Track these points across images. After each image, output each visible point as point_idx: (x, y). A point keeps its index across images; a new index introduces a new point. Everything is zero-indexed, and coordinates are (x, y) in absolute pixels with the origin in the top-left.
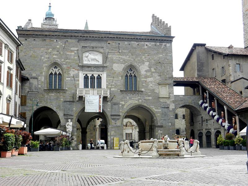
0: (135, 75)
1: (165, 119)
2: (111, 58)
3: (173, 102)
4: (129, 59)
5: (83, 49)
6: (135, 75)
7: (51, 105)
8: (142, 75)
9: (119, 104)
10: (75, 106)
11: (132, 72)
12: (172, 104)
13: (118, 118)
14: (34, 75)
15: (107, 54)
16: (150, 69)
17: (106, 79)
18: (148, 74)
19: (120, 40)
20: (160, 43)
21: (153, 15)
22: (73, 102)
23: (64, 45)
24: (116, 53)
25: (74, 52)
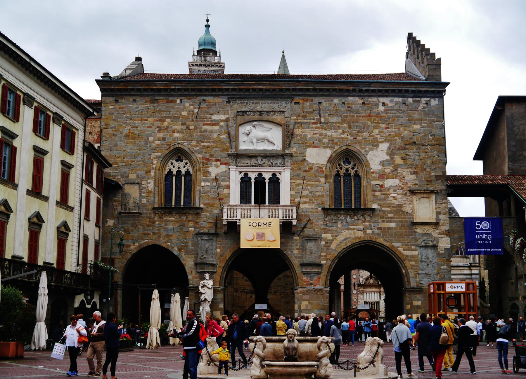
0: (356, 171)
1: (426, 274)
2: (301, 135)
3: (448, 233)
5: (239, 118)
7: (168, 241)
9: (321, 239)
10: (221, 244)
11: (351, 166)
12: (444, 239)
13: (316, 270)
14: (132, 176)
15: (291, 127)
16: (392, 158)
17: (291, 183)
19: (322, 96)
20: (414, 99)
21: (410, 35)
22: (216, 234)
23: (196, 111)
24: (313, 123)
25: (218, 124)
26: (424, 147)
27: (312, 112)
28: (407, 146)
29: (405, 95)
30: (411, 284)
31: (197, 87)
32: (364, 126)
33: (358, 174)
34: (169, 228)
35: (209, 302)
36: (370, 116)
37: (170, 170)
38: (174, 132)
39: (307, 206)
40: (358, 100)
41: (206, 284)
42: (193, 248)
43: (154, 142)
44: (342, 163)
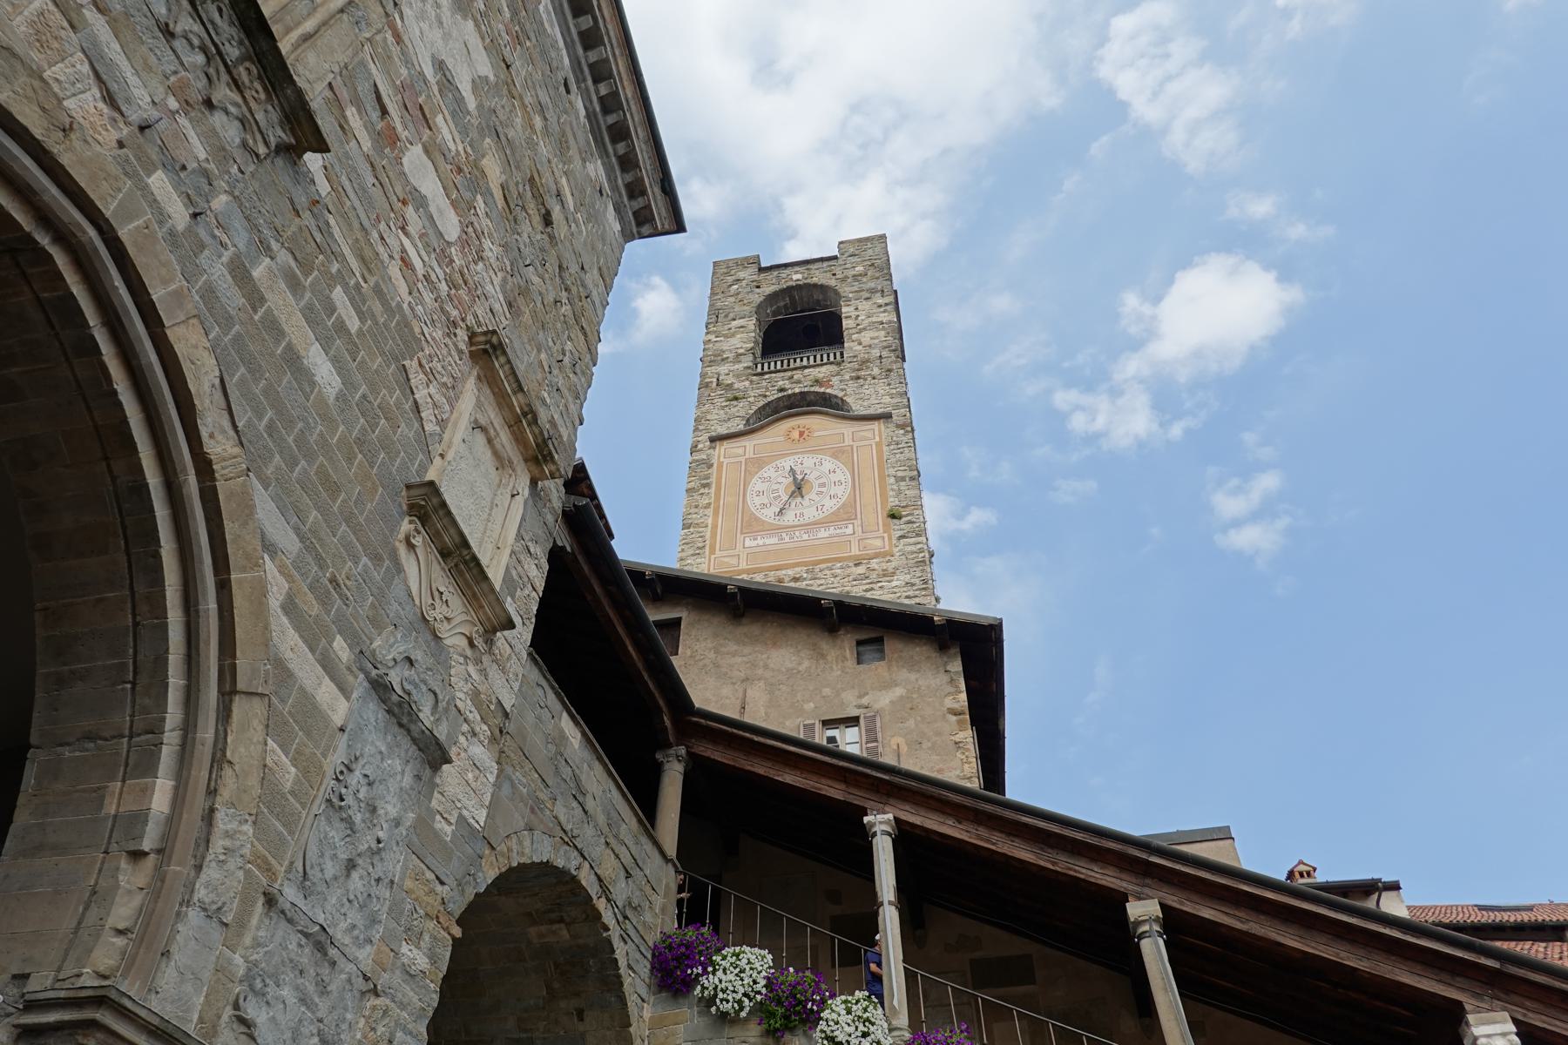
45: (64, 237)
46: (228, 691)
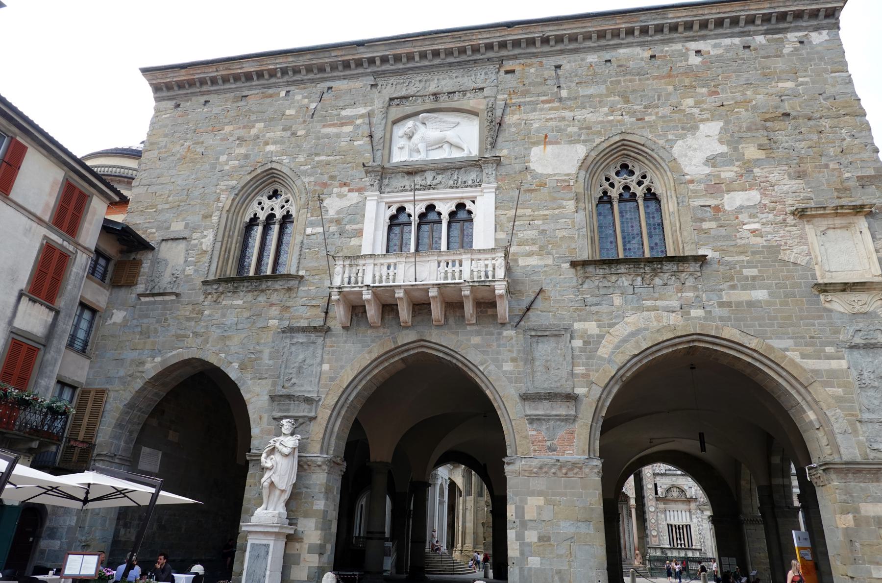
0: (649, 190)
4: (608, 119)
6: (649, 190)
8: (692, 182)
14: (177, 227)
16: (736, 149)
18: (728, 173)
19: (562, 52)
20: (770, 36)
22: (324, 330)
24: (543, 102)
26: (811, 123)
27: (540, 84)
28: (768, 124)
29: (746, 29)
30: (842, 450)
31: (315, 62)
32: (659, 97)
33: (654, 194)
34: (228, 323)
35: (283, 491)
36: (670, 76)
37: (255, 214)
38: (266, 143)
39: (533, 261)
40: (640, 52)
41: (277, 445)
42: (271, 362)
43: (227, 164)
44: (613, 174)
45: (693, 341)
46: (806, 387)
